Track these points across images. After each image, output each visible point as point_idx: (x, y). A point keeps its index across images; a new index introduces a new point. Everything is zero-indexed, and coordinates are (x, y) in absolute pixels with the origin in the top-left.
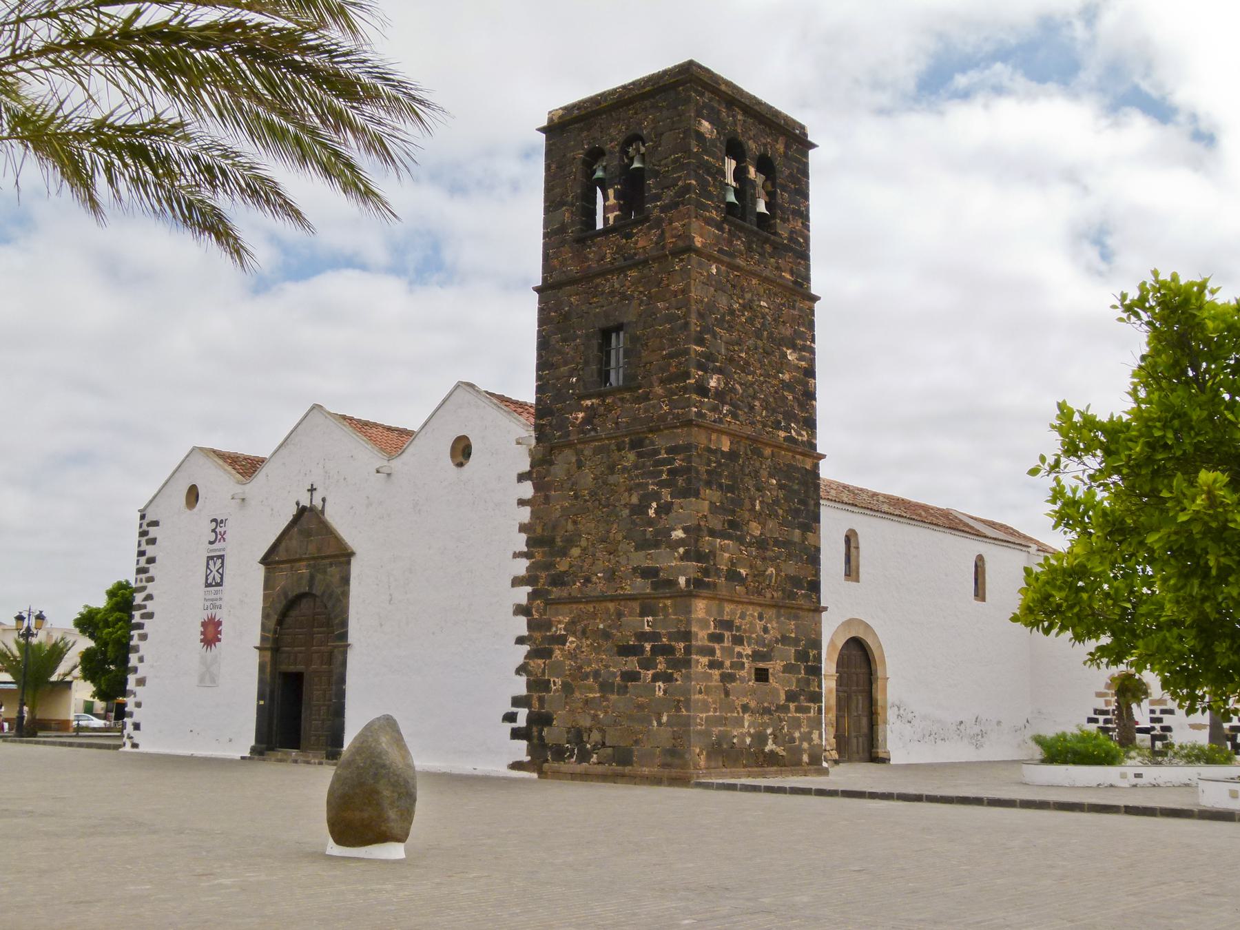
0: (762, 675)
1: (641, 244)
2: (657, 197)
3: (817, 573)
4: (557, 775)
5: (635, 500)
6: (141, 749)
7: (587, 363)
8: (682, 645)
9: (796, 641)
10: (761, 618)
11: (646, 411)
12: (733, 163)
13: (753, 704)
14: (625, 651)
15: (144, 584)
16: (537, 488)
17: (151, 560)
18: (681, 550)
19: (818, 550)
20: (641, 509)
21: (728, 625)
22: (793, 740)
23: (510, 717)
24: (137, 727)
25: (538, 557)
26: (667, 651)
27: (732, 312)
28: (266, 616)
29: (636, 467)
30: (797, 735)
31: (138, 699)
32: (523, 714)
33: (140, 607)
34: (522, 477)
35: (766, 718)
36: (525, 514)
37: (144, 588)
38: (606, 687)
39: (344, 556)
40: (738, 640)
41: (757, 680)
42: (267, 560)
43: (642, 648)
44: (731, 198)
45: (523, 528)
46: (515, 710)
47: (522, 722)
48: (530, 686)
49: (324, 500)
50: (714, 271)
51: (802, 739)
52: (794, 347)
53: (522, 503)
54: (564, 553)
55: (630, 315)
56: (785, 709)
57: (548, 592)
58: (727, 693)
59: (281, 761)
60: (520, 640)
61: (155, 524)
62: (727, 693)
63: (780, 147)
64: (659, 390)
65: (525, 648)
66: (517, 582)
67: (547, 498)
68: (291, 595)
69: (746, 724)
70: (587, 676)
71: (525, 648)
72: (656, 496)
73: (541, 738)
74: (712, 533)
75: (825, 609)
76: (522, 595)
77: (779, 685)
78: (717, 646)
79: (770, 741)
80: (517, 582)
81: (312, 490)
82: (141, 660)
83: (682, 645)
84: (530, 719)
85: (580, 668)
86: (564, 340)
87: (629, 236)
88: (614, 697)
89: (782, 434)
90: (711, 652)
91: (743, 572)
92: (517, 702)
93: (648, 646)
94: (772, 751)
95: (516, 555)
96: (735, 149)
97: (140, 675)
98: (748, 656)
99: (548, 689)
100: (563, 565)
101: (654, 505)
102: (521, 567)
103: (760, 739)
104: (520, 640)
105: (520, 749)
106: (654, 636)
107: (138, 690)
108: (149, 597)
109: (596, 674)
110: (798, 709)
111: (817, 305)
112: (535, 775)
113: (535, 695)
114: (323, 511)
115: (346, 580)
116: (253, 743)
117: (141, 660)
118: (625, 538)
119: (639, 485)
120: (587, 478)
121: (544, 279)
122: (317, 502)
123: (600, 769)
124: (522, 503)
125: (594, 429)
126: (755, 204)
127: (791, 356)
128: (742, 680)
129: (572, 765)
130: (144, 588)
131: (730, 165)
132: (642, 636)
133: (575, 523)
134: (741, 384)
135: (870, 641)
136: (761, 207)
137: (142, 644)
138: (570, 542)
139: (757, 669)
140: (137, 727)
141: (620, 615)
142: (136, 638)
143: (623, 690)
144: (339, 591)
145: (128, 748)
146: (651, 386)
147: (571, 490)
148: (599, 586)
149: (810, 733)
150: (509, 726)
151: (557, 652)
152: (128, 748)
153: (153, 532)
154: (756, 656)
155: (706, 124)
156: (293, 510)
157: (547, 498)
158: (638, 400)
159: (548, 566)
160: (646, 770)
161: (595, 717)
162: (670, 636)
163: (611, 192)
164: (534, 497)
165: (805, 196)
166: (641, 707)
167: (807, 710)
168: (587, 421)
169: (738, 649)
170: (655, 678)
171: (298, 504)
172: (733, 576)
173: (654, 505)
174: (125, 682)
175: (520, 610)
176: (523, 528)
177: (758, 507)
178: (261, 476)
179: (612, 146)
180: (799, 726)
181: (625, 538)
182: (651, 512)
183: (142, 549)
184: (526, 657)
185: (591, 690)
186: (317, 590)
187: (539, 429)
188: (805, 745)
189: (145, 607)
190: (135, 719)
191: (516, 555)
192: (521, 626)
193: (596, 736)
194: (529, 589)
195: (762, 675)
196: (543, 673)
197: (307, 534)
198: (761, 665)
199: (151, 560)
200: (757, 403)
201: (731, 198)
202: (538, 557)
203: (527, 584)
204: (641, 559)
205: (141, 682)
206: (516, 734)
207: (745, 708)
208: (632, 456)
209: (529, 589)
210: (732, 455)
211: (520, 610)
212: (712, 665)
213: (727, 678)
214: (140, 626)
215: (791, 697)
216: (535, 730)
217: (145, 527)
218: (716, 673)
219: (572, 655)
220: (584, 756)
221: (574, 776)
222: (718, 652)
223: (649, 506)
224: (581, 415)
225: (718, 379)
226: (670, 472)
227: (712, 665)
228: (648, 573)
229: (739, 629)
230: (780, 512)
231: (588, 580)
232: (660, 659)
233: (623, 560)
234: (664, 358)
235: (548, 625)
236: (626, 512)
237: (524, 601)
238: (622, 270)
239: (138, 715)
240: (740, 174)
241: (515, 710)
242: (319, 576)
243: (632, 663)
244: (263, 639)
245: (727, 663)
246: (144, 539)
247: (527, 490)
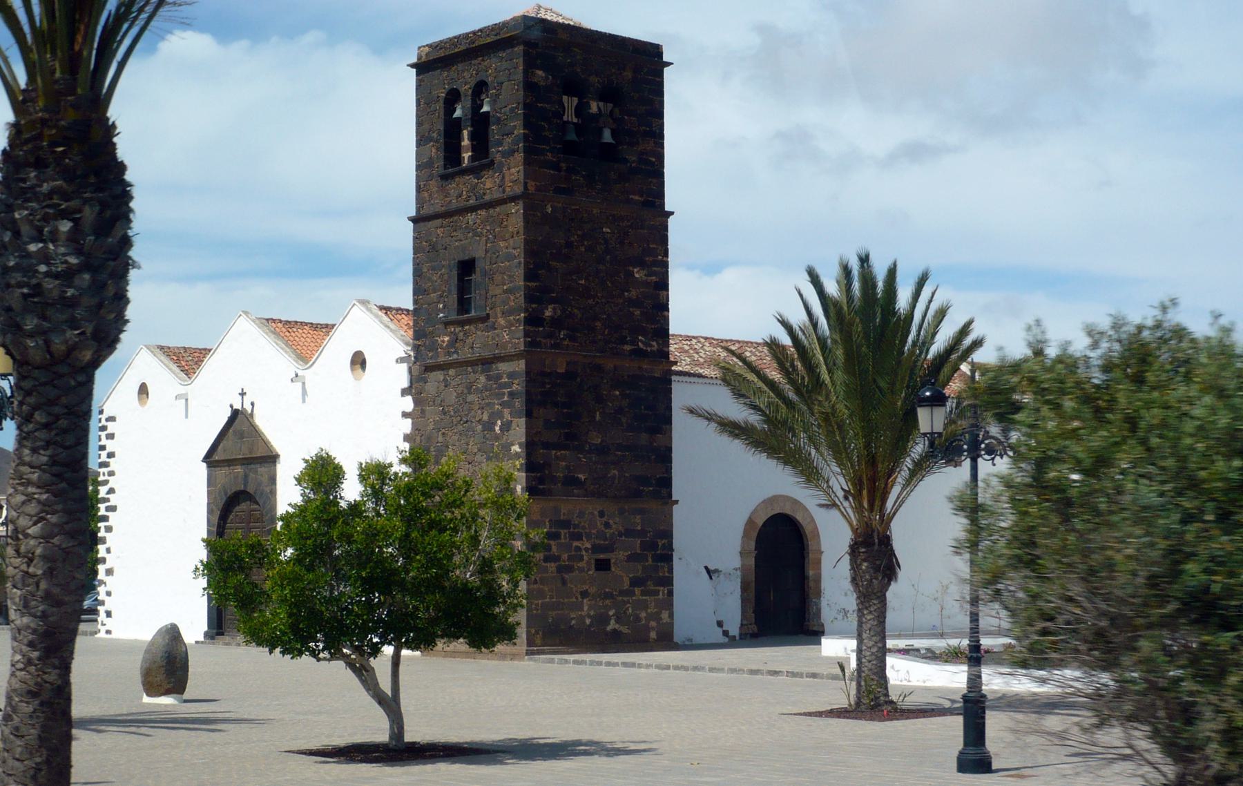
0: (603, 565)
2: (500, 143)
3: (669, 470)
5: (485, 417)
6: (113, 636)
7: (450, 291)
9: (642, 533)
10: (602, 514)
11: (493, 339)
12: (575, 100)
13: (592, 590)
15: (106, 478)
16: (416, 402)
17: (111, 455)
19: (670, 450)
20: (489, 426)
21: (566, 524)
22: (638, 619)
24: (109, 614)
27: (569, 245)
28: (210, 512)
29: (486, 388)
30: (643, 615)
31: (108, 588)
33: (105, 500)
34: (404, 392)
35: (607, 602)
37: (106, 482)
40: (578, 537)
41: (597, 569)
42: (209, 458)
44: (572, 136)
45: (407, 438)
49: (252, 404)
50: (549, 210)
51: (649, 618)
52: (642, 264)
53: (405, 415)
55: (478, 251)
56: (630, 593)
58: (564, 582)
59: (227, 644)
61: (111, 419)
62: (564, 582)
63: (628, 74)
64: (502, 321)
67: (423, 412)
68: (229, 493)
69: (586, 608)
74: (547, 446)
75: (677, 502)
77: (622, 573)
78: (552, 542)
79: (613, 622)
81: (243, 394)
82: (108, 551)
86: (433, 269)
89: (628, 348)
90: (548, 548)
91: (582, 477)
94: (615, 630)
96: (573, 87)
97: (108, 565)
98: (587, 550)
101: (499, 423)
103: (602, 619)
107: (107, 579)
108: (111, 491)
110: (643, 593)
111: (671, 220)
114: (252, 415)
116: (205, 628)
117: (108, 551)
119: (488, 404)
120: (451, 396)
121: (418, 210)
122: (248, 408)
124: (405, 415)
125: (456, 352)
126: (600, 133)
127: (638, 274)
128: (581, 570)
130: (106, 482)
131: (570, 103)
134: (579, 309)
135: (799, 517)
136: (607, 136)
137: (108, 535)
139: (597, 560)
140: (109, 614)
142: (103, 530)
144: (267, 490)
145: (102, 635)
146: (496, 317)
149: (659, 613)
153: (111, 427)
154: (596, 549)
155: (540, 73)
156: (228, 413)
157: (423, 412)
158: (487, 329)
163: (465, 133)
165: (660, 115)
167: (657, 593)
169: (576, 544)
172: (571, 481)
173: (499, 423)
174: (96, 573)
177: (598, 417)
178: (210, 366)
179: (466, 89)
180: (646, 608)
182: (497, 428)
183: (102, 443)
186: (250, 489)
187: (416, 348)
188: (653, 624)
190: (107, 607)
195: (603, 565)
197: (241, 435)
198: (602, 556)
199: (111, 455)
200: (598, 324)
201: (572, 136)
205: (109, 572)
207: (584, 594)
208: (483, 379)
210: (570, 375)
212: (546, 559)
213: (560, 570)
214: (105, 519)
215: (635, 582)
217: (103, 422)
218: (552, 566)
222: (554, 549)
223: (495, 424)
224: (446, 339)
225: (554, 309)
227: (546, 559)
229: (576, 526)
230: (624, 420)
234: (505, 292)
238: (473, 209)
239: (110, 604)
240: (579, 111)
242: (252, 475)
244: (209, 532)
245: (565, 556)
246: (103, 434)
247: (408, 404)
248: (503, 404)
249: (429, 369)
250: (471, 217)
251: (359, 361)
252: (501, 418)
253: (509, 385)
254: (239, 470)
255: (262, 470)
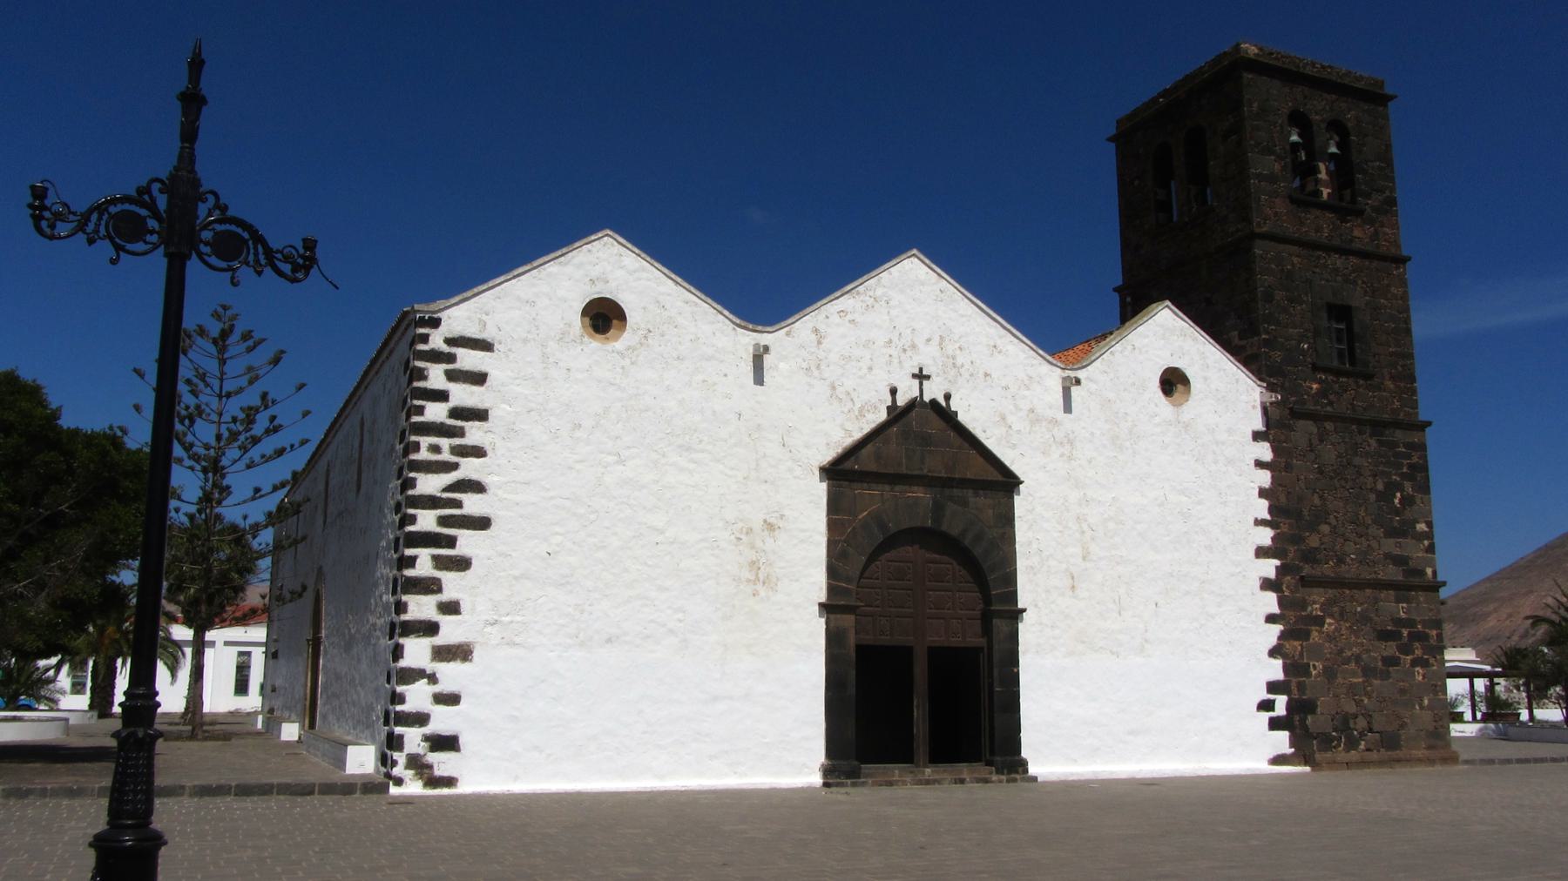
1: (1357, 233)
2: (1368, 196)
4: (1333, 764)
5: (1380, 487)
6: (463, 788)
8: (1434, 633)
14: (1385, 636)
18: (1426, 543)
20: (1386, 496)
23: (1266, 706)
25: (1285, 529)
26: (1422, 637)
32: (1281, 702)
34: (1257, 436)
36: (1265, 478)
38: (1368, 672)
39: (1008, 483)
43: (1400, 634)
45: (1263, 493)
46: (1271, 697)
47: (1281, 708)
48: (1286, 669)
49: (948, 397)
53: (1259, 464)
54: (1313, 527)
55: (1357, 298)
57: (1300, 569)
60: (1271, 619)
64: (1389, 384)
65: (1277, 629)
66: (1261, 552)
67: (1288, 467)
68: (893, 527)
70: (1347, 661)
71: (1277, 629)
72: (1400, 488)
73: (1306, 728)
76: (1269, 567)
80: (1261, 552)
83: (1434, 633)
84: (1289, 707)
85: (1341, 651)
87: (1344, 221)
88: (1376, 682)
92: (1273, 687)
93: (1405, 633)
95: (1258, 522)
99: (1308, 674)
100: (1314, 541)
102: (1265, 536)
104: (1271, 619)
105: (1281, 741)
106: (1409, 623)
109: (1358, 658)
112: (1308, 769)
113: (1294, 681)
115: (1008, 519)
118: (1374, 522)
120: (1329, 453)
123: (1374, 755)
125: (1331, 403)
129: (1341, 754)
132: (1399, 622)
133: (1321, 497)
138: (1321, 516)
141: (1376, 601)
143: (1385, 675)
147: (1314, 462)
148: (1350, 570)
150: (1266, 716)
151: (1315, 634)
152: (413, 787)
159: (1296, 539)
160: (1419, 753)
161: (1358, 703)
162: (1424, 623)
163: (1322, 166)
164: (1273, 461)
166: (1403, 691)
168: (1322, 393)
170: (1414, 663)
171: (894, 391)
175: (1267, 585)
176: (1263, 493)
181: (1374, 522)
184: (1279, 638)
185: (1354, 674)
189: (458, 504)
191: (1258, 522)
192: (1270, 602)
193: (1362, 723)
194: (1277, 562)
196: (1301, 654)
202: (1285, 529)
203: (1274, 557)
204: (1390, 545)
206: (1275, 724)
208: (1373, 442)
209: (1277, 562)
211: (1267, 585)
216: (1297, 718)
219: (1330, 638)
220: (1352, 744)
221: (1349, 765)
226: (1411, 466)
228: (1400, 561)
231: (1341, 561)
232: (1417, 644)
233: (1374, 544)
234: (1391, 354)
235: (1303, 604)
236: (1373, 497)
237: (1272, 574)
241: (1271, 697)
243: (1390, 649)
247: (1265, 452)
248: (1403, 476)
249: (1296, 414)
250: (1337, 261)
251: (1173, 382)
252: (1402, 490)
253: (1409, 457)
254: (919, 493)
255: (981, 503)
